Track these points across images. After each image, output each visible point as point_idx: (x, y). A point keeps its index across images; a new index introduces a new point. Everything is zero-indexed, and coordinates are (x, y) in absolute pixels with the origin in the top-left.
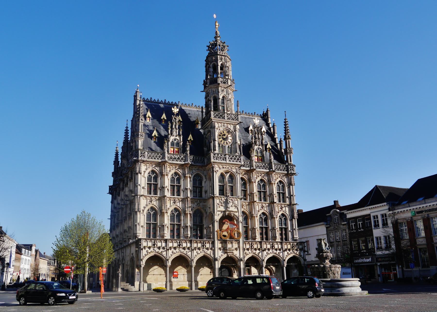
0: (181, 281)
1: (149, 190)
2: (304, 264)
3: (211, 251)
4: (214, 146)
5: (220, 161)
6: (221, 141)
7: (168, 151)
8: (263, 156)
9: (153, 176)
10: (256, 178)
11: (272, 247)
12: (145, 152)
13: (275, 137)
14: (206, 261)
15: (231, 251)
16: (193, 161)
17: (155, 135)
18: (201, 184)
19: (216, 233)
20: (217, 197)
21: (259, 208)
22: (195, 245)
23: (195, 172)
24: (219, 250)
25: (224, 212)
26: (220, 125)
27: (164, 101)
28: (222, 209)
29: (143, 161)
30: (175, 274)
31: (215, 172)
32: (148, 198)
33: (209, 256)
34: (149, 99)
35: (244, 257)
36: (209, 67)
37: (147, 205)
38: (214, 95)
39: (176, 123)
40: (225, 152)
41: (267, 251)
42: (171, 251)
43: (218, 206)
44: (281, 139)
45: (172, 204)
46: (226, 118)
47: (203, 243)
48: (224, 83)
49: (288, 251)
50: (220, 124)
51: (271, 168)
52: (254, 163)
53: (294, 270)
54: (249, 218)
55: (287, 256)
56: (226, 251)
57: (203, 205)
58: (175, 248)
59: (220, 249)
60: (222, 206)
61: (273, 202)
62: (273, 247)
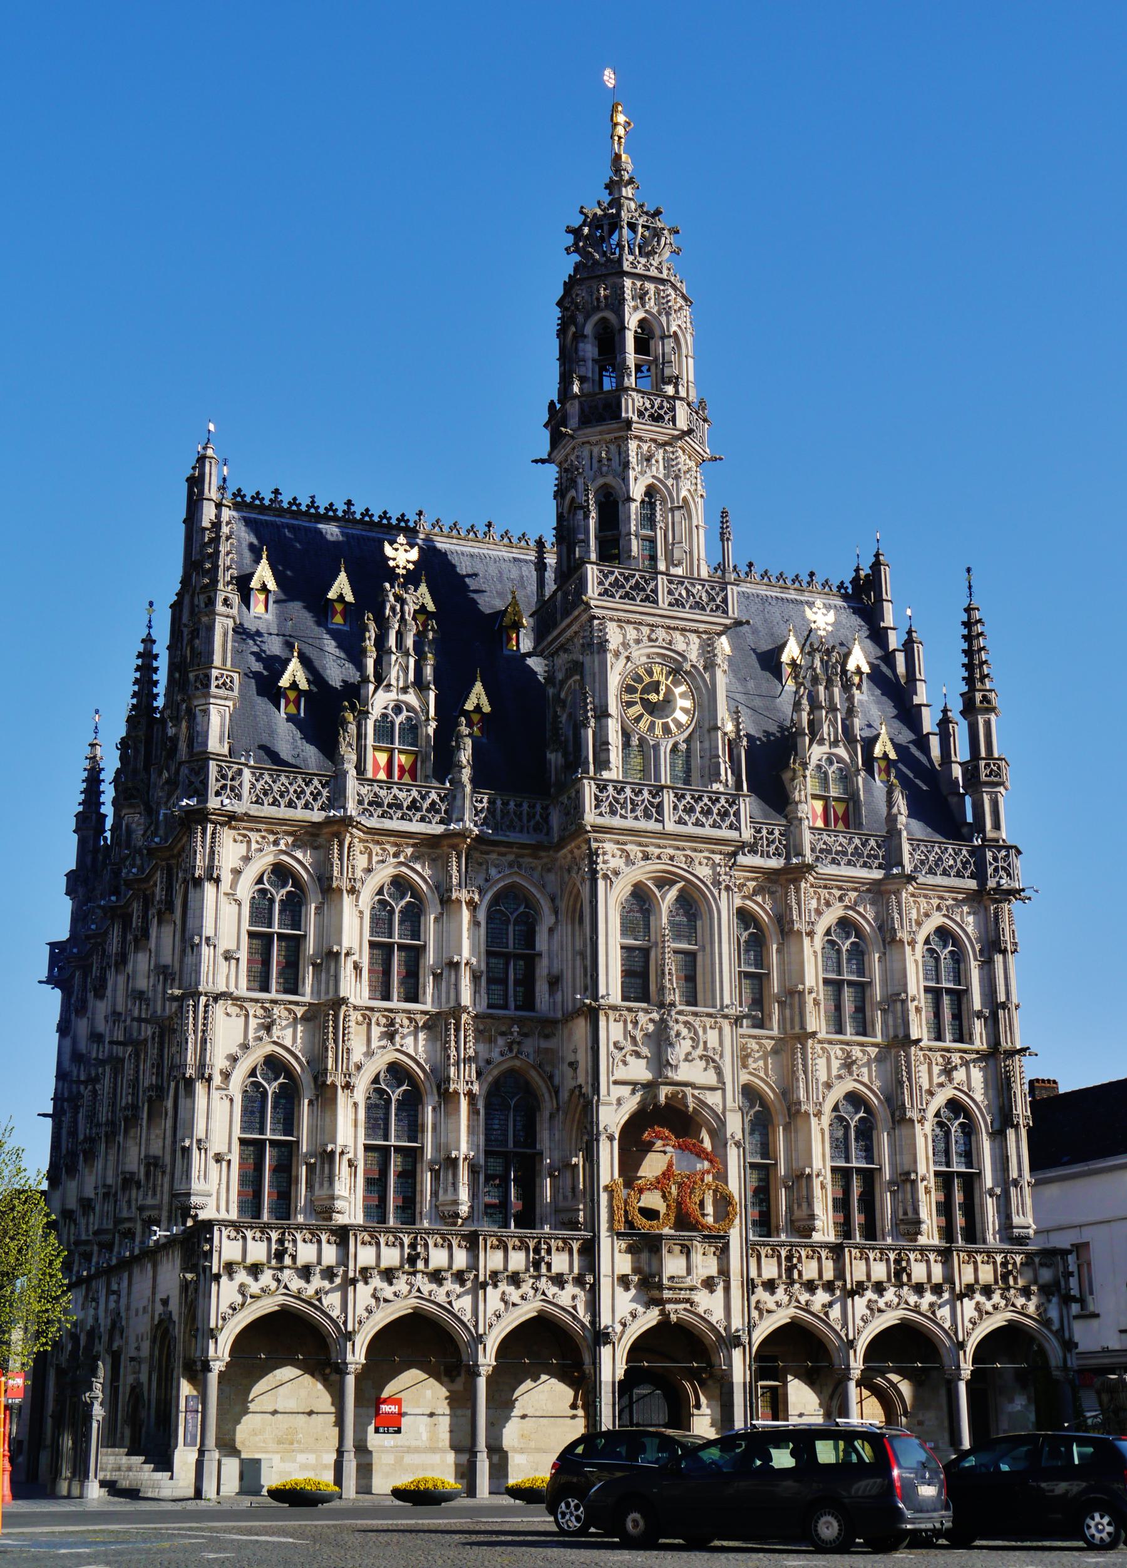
0: (417, 1450)
1: (258, 967)
2: (1065, 1368)
3: (577, 1291)
4: (602, 745)
6: (638, 719)
7: (360, 769)
8: (851, 799)
9: (280, 895)
10: (818, 913)
11: (898, 1274)
12: (240, 772)
13: (917, 700)
14: (549, 1346)
15: (683, 1295)
16: (491, 818)
17: (294, 685)
18: (529, 937)
19: (604, 1198)
20: (614, 1008)
21: (834, 1071)
22: (493, 1260)
23: (500, 879)
24: (619, 1290)
25: (650, 1087)
26: (631, 633)
27: (341, 508)
28: (639, 1070)
29: (231, 819)
30: (385, 1408)
31: (606, 877)
32: (253, 1009)
33: (568, 1319)
34: (268, 496)
35: (751, 1327)
36: (579, 336)
37: (245, 1047)
38: (601, 481)
39: (403, 620)
40: (657, 778)
42: (369, 1289)
43: (618, 1055)
44: (945, 711)
45: (375, 1044)
46: (663, 599)
47: (537, 1250)
48: (657, 418)
49: (978, 1297)
50: (630, 628)
51: (892, 859)
52: (807, 837)
53: (1011, 1401)
54: (780, 1120)
55: (973, 1322)
56: (655, 1293)
57: (538, 1051)
58: (389, 1275)
59: (624, 1281)
60: (638, 1055)
61: (902, 1041)
62: (899, 1274)
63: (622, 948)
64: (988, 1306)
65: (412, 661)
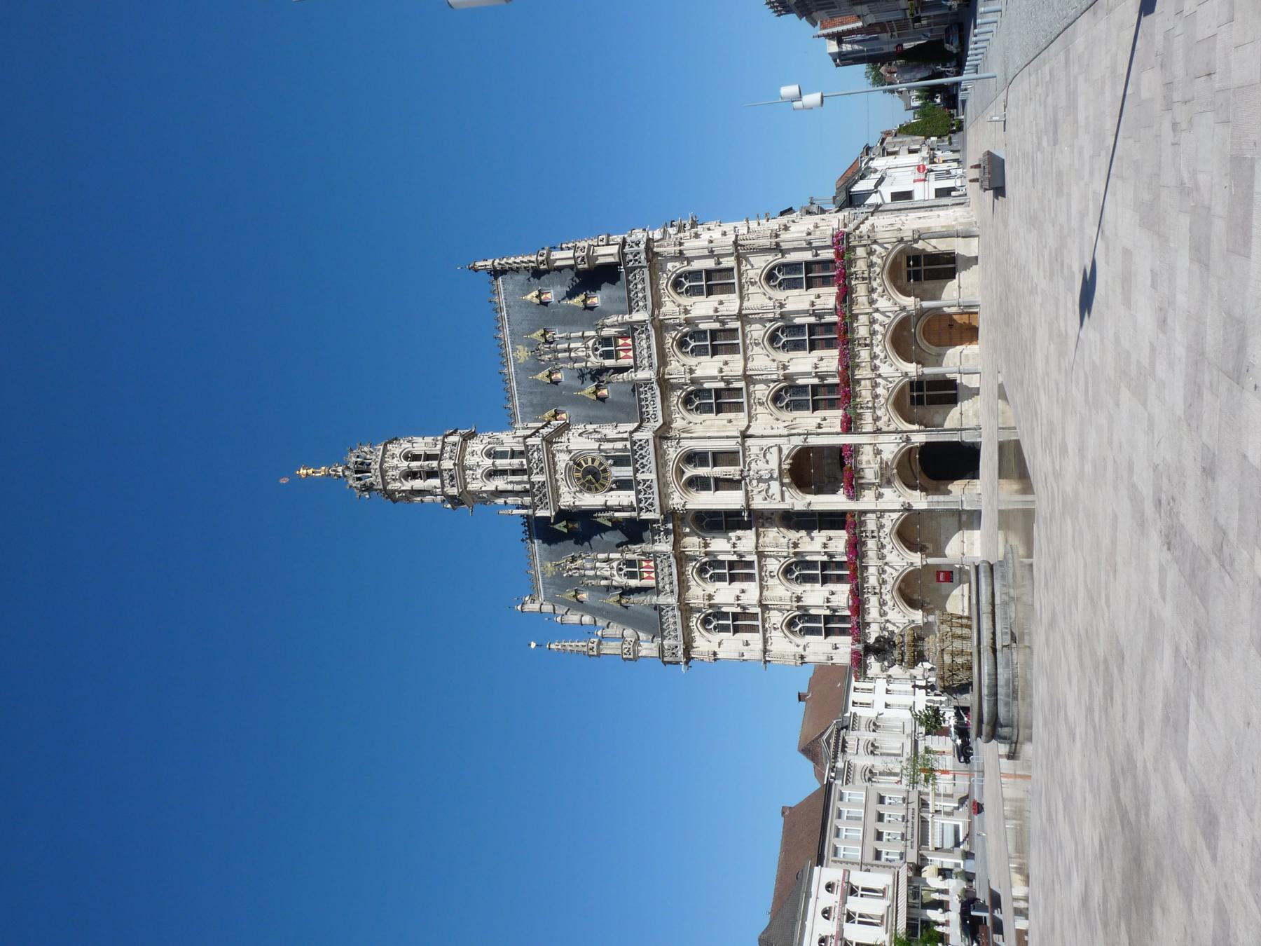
5: (656, 496)
24: (885, 498)
25: (782, 485)
26: (563, 489)
28: (775, 486)
41: (877, 362)
46: (542, 478)
63: (717, 489)
64: (880, 289)
65: (598, 564)
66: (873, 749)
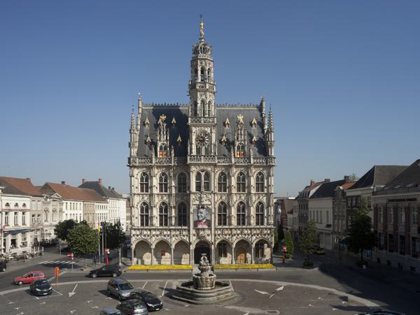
4: (191, 149)
7: (156, 155)
10: (235, 172)
23: (179, 171)
26: (197, 128)
28: (197, 202)
35: (215, 241)
46: (202, 122)
59: (194, 235)
61: (249, 193)
66: (54, 211)
